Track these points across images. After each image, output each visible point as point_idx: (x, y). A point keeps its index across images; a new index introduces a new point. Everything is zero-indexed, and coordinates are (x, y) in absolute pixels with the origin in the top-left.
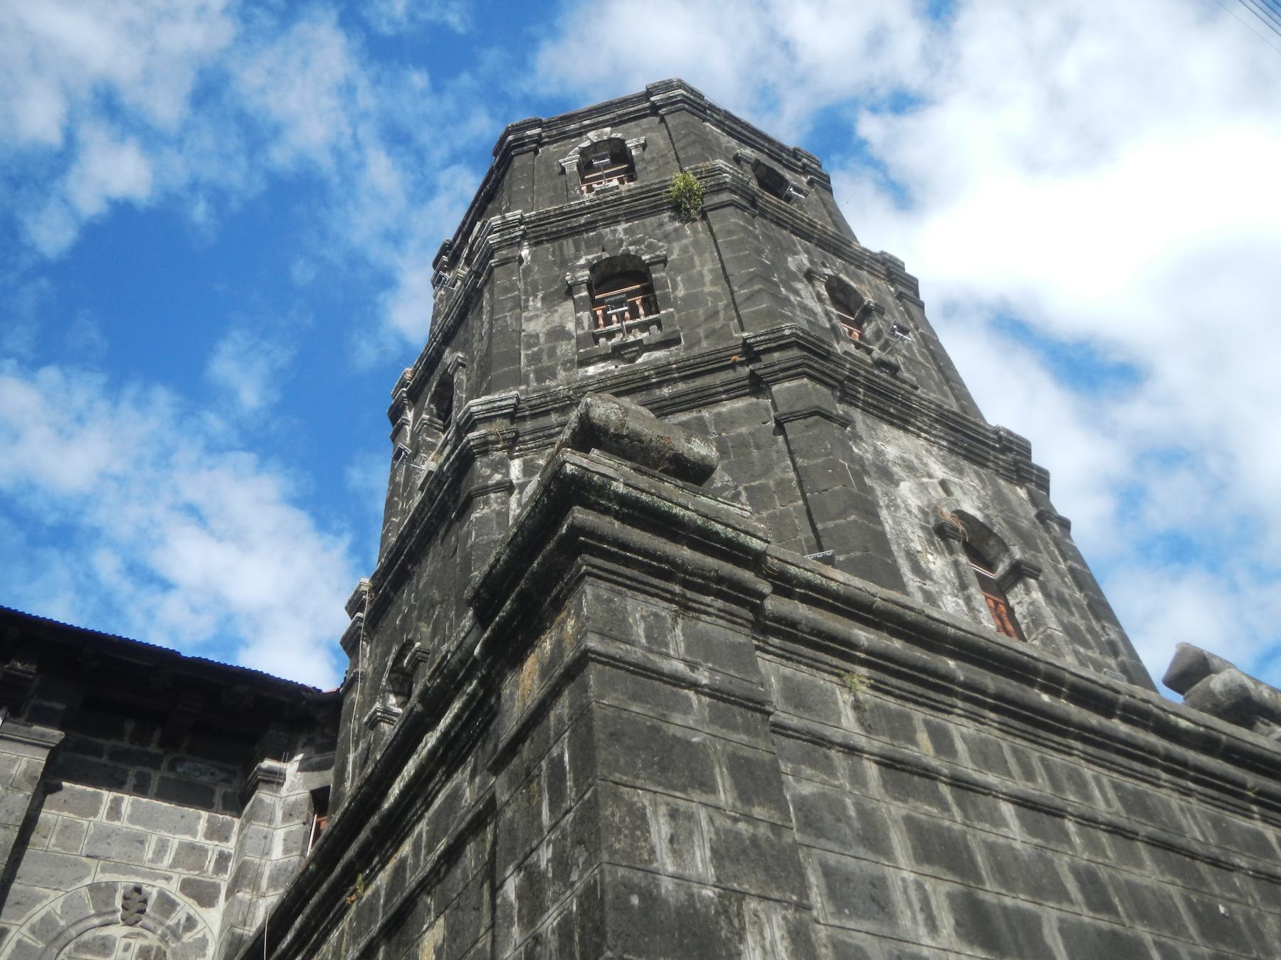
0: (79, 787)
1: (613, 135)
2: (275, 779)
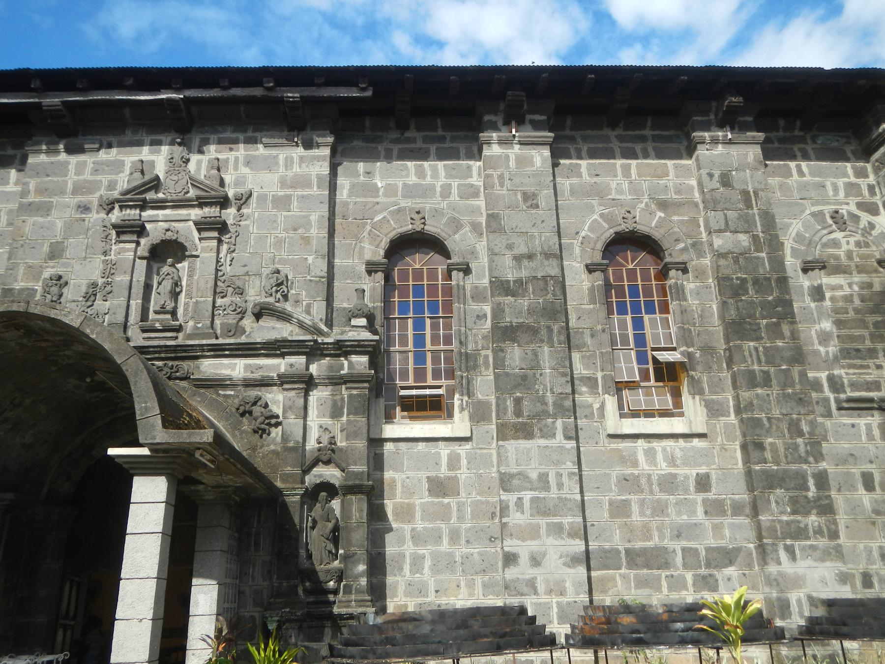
0: (775, 163)
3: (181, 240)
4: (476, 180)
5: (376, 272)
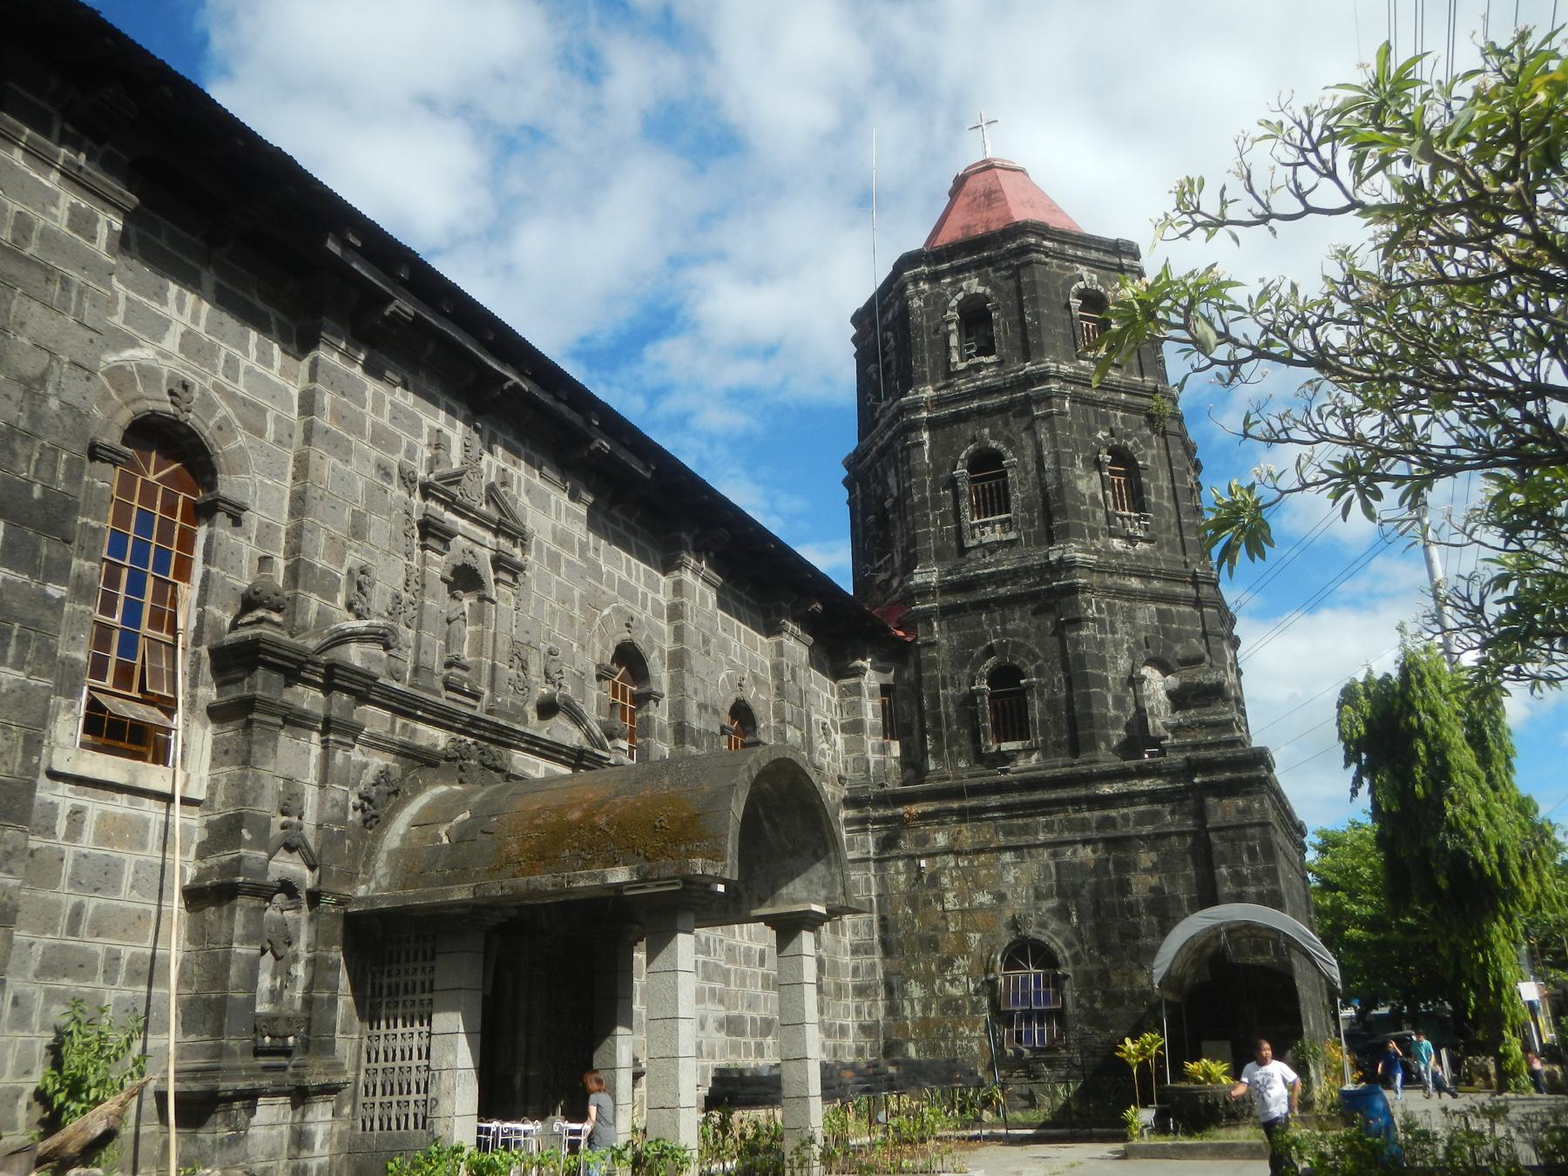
2: (859, 672)
3: (481, 572)
4: (664, 598)
5: (606, 679)
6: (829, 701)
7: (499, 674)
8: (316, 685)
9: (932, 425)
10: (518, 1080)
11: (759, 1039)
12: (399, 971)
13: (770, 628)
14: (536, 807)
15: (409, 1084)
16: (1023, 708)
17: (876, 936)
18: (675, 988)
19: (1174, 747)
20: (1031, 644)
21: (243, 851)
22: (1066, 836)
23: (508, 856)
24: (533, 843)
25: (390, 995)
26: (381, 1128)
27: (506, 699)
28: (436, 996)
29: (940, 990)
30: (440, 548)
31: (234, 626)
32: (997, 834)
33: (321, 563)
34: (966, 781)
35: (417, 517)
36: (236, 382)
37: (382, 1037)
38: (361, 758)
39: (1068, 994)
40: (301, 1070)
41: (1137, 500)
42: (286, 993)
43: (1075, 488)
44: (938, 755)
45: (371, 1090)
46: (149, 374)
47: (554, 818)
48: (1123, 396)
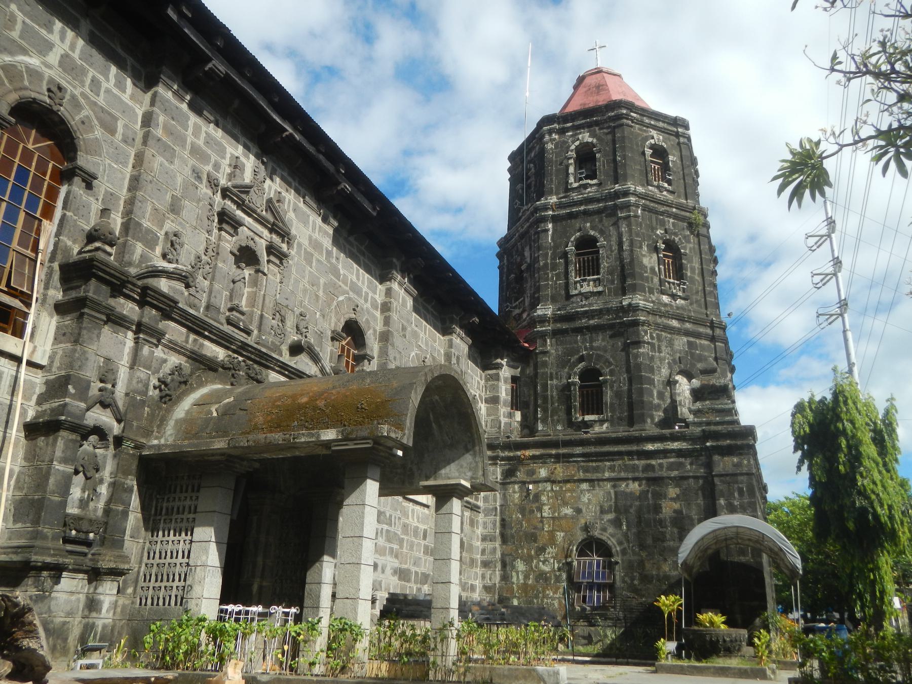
1: (663, 144)
2: (499, 367)
3: (258, 253)
4: (380, 298)
5: (337, 340)
6: (478, 383)
7: (264, 321)
8: (134, 300)
9: (555, 219)
10: (255, 588)
11: (419, 586)
12: (175, 498)
13: (445, 331)
14: (278, 395)
15: (174, 575)
16: (600, 395)
17: (498, 531)
18: (362, 517)
19: (694, 423)
20: (608, 356)
21: (67, 400)
22: (623, 475)
23: (255, 425)
24: (274, 417)
25: (167, 514)
26: (152, 604)
27: (268, 338)
28: (197, 516)
29: (536, 567)
30: (232, 232)
31: (80, 253)
32: (579, 471)
33: (146, 223)
34: (561, 437)
35: (217, 209)
36: (98, 96)
37: (159, 543)
38: (162, 355)
39: (617, 573)
40: (96, 557)
41: (679, 273)
42: (92, 504)
43: (642, 262)
44: (544, 421)
45: (148, 577)
46: (34, 74)
47: (289, 401)
48: (674, 210)
